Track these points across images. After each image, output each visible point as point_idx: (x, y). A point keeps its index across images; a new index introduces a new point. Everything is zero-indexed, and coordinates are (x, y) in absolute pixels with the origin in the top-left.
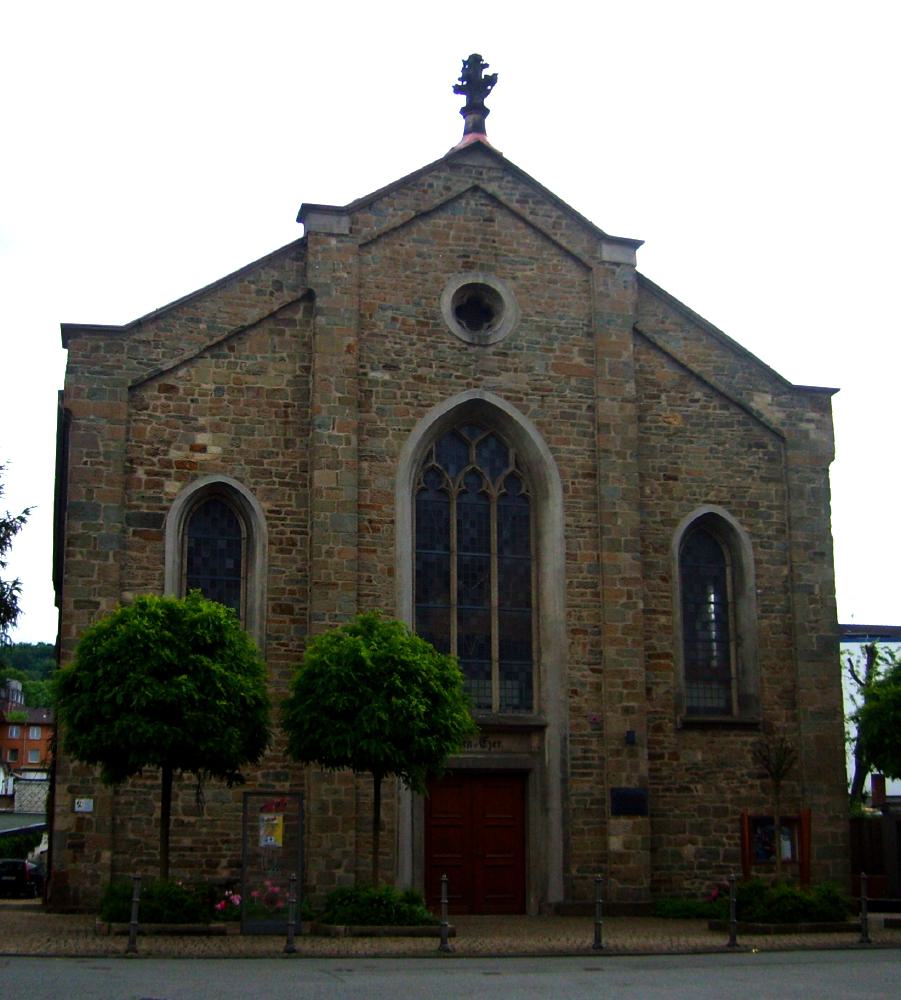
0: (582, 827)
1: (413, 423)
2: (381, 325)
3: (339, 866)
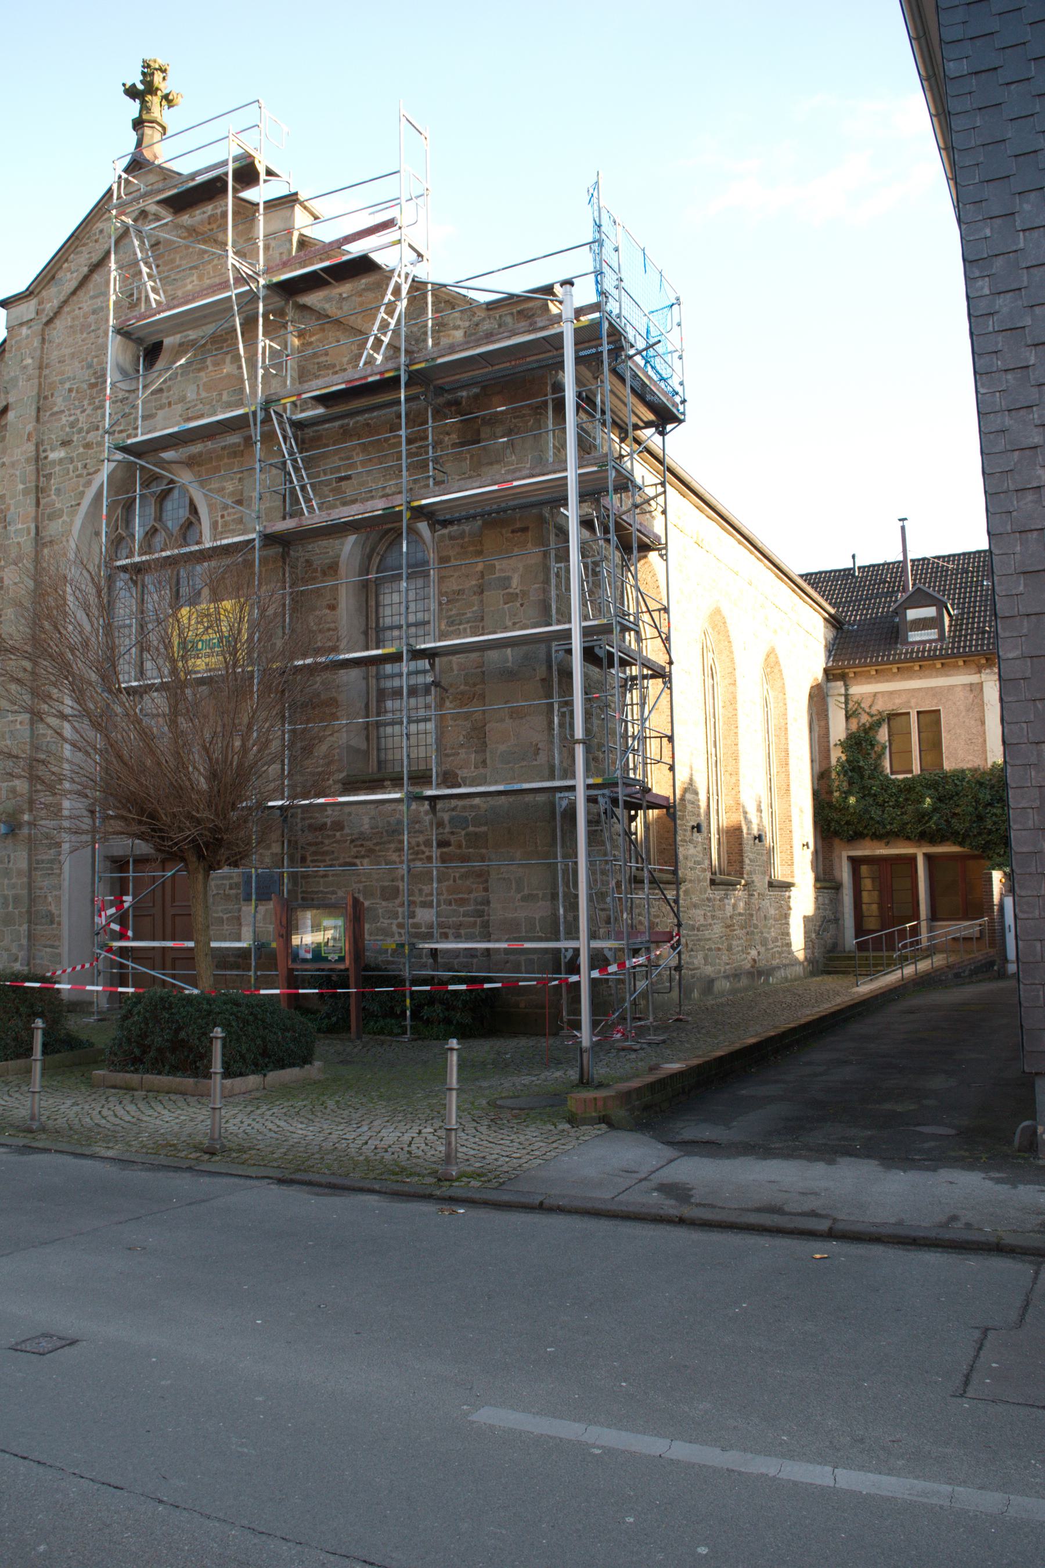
0: (221, 915)
1: (82, 493)
2: (59, 400)
3: (16, 960)
